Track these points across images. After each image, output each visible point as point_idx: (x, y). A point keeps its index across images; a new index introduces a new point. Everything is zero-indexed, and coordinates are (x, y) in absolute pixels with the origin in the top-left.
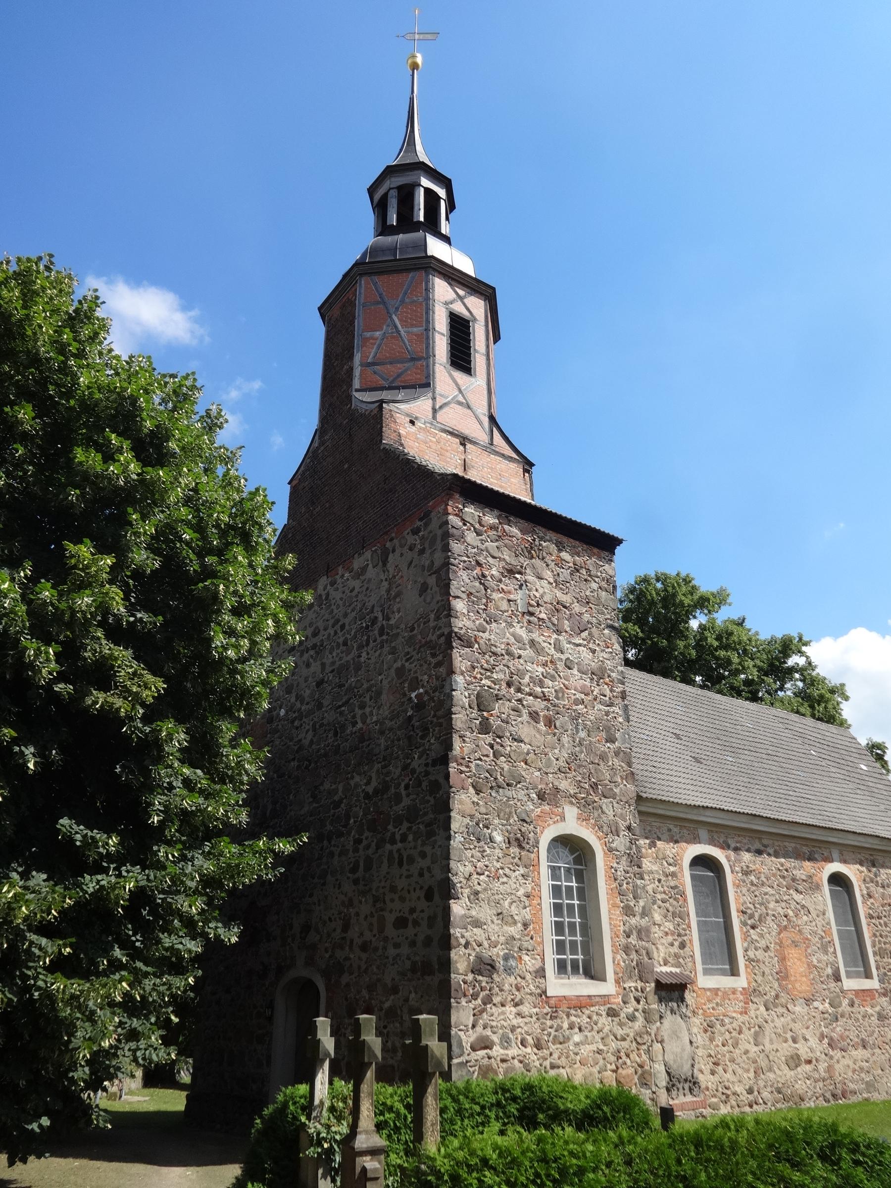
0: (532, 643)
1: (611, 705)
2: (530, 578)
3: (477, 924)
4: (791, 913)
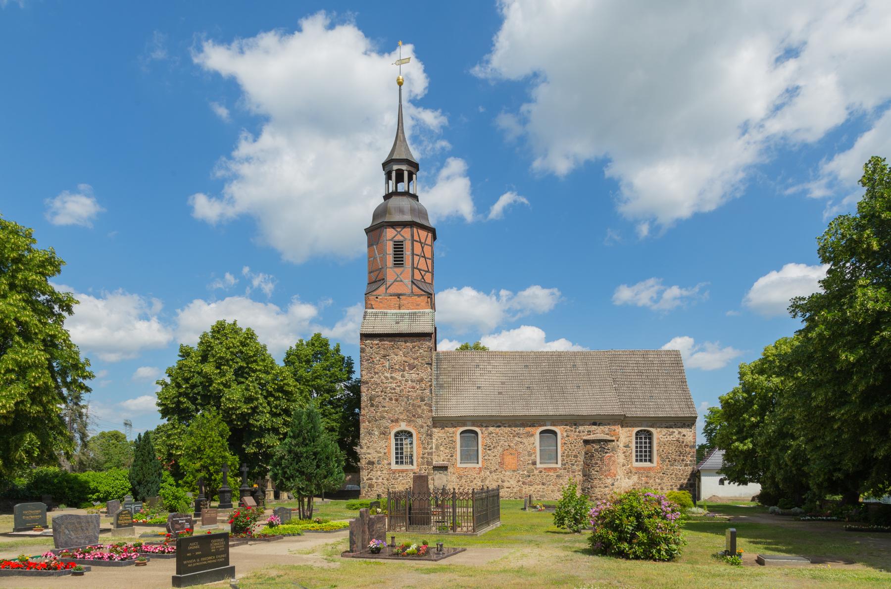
0: (392, 377)
1: (425, 390)
2: (393, 356)
3: (369, 454)
4: (512, 444)
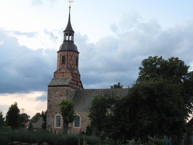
0: (56, 99)
